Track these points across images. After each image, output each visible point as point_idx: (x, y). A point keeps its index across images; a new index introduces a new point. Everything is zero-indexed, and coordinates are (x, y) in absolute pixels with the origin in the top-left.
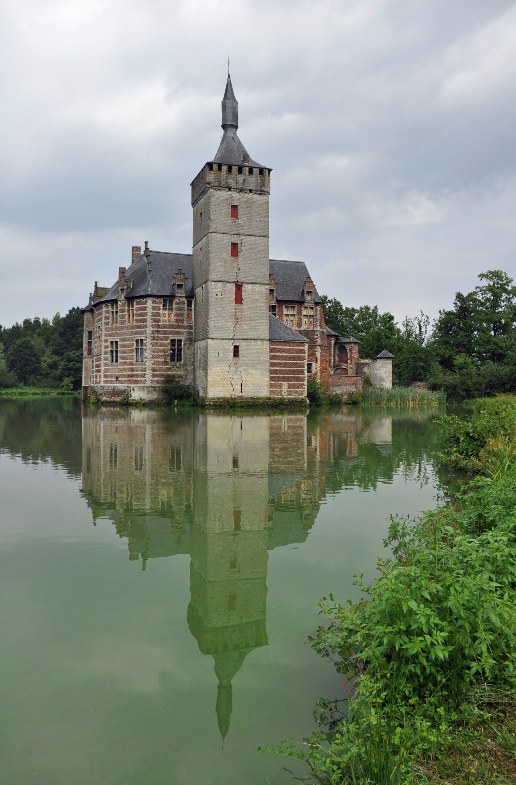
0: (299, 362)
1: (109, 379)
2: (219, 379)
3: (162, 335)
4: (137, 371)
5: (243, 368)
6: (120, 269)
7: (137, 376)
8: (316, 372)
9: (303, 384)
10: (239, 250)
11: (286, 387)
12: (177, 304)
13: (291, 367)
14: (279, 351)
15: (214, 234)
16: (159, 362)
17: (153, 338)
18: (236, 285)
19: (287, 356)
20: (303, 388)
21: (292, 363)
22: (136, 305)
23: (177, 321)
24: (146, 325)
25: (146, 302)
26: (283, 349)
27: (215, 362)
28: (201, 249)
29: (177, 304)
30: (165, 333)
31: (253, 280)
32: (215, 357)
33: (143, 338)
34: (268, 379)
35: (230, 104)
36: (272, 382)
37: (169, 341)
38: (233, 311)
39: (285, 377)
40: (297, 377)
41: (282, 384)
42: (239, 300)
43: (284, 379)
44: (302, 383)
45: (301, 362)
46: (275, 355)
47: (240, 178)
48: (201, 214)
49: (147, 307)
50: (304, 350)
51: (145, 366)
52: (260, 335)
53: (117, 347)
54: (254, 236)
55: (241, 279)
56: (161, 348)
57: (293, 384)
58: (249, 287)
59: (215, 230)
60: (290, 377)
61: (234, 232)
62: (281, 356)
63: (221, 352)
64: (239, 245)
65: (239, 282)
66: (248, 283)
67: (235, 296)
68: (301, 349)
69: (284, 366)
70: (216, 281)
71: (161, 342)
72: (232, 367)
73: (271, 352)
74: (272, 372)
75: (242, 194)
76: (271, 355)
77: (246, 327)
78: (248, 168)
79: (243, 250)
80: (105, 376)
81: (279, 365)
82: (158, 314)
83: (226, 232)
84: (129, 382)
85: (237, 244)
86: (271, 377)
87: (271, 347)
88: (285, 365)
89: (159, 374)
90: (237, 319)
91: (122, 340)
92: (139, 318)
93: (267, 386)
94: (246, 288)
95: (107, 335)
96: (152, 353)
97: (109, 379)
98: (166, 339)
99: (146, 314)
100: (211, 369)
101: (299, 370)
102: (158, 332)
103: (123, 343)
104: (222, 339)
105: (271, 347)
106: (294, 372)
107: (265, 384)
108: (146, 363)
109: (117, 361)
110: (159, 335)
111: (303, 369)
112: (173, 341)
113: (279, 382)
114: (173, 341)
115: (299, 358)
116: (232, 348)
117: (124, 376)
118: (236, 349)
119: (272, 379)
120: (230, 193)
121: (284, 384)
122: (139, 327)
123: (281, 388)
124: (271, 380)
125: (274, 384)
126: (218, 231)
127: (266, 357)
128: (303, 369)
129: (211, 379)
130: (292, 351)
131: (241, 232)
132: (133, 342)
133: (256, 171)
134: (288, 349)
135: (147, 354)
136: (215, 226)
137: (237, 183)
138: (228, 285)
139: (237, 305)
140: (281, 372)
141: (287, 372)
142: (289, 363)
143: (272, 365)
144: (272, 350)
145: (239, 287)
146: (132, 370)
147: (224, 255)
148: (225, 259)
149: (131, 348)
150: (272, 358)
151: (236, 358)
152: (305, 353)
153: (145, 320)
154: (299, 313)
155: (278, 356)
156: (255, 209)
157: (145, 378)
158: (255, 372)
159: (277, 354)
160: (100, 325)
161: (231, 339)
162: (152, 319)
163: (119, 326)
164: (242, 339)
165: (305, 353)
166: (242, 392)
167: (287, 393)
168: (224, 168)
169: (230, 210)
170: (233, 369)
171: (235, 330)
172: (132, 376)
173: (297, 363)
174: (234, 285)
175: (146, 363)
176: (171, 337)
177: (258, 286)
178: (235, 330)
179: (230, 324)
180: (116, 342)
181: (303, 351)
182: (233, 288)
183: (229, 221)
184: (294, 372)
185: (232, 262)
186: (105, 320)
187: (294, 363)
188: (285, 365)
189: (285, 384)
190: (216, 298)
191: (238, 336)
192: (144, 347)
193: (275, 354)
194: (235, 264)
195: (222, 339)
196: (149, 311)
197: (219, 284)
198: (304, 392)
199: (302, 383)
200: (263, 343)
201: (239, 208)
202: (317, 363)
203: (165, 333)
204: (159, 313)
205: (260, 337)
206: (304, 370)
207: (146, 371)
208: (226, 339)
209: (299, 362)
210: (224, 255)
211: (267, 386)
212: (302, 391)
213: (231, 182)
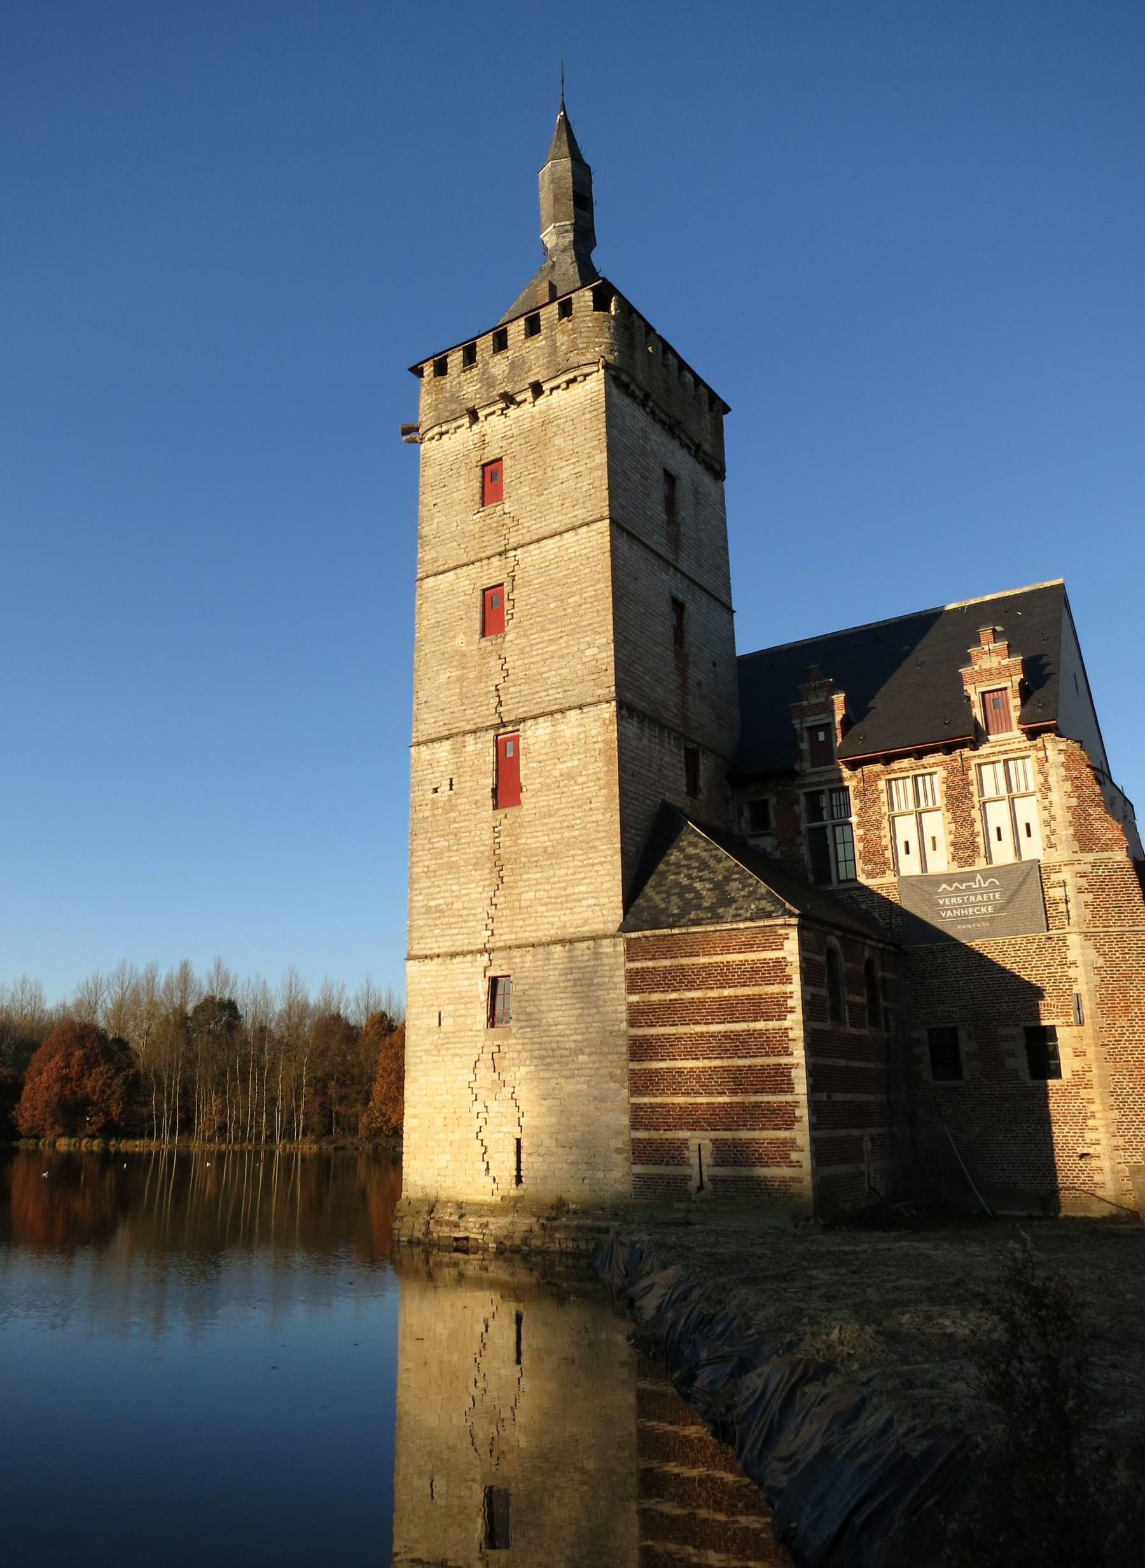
2: (439, 1122)
9: (791, 1144)
10: (507, 605)
15: (431, 580)
19: (702, 1001)
20: (791, 1164)
26: (682, 967)
27: (426, 1051)
31: (552, 697)
32: (429, 1030)
34: (626, 1120)
38: (487, 836)
40: (757, 1105)
41: (685, 1142)
44: (783, 1134)
45: (772, 1024)
46: (650, 1004)
50: (780, 965)
52: (586, 921)
58: (540, 732)
61: (489, 553)
63: (447, 1009)
64: (507, 588)
66: (535, 717)
68: (764, 962)
70: (433, 741)
76: (630, 1005)
77: (531, 895)
86: (636, 1108)
101: (763, 1068)
104: (453, 955)
111: (784, 1060)
115: (757, 1008)
116: (483, 986)
125: (650, 1142)
126: (441, 569)
128: (784, 1060)
137: (488, 381)
142: (713, 1035)
147: (460, 638)
148: (464, 655)
152: (788, 980)
155: (660, 1004)
156: (558, 441)
159: (656, 997)
161: (481, 952)
164: (518, 947)
165: (788, 980)
167: (708, 1185)
170: (486, 1075)
171: (492, 911)
177: (573, 715)
178: (492, 911)
183: (474, 521)
185: (483, 655)
190: (434, 802)
191: (505, 936)
193: (646, 997)
194: (494, 663)
195: (453, 955)
201: (507, 462)
205: (586, 930)
210: (460, 641)
211: (618, 1151)
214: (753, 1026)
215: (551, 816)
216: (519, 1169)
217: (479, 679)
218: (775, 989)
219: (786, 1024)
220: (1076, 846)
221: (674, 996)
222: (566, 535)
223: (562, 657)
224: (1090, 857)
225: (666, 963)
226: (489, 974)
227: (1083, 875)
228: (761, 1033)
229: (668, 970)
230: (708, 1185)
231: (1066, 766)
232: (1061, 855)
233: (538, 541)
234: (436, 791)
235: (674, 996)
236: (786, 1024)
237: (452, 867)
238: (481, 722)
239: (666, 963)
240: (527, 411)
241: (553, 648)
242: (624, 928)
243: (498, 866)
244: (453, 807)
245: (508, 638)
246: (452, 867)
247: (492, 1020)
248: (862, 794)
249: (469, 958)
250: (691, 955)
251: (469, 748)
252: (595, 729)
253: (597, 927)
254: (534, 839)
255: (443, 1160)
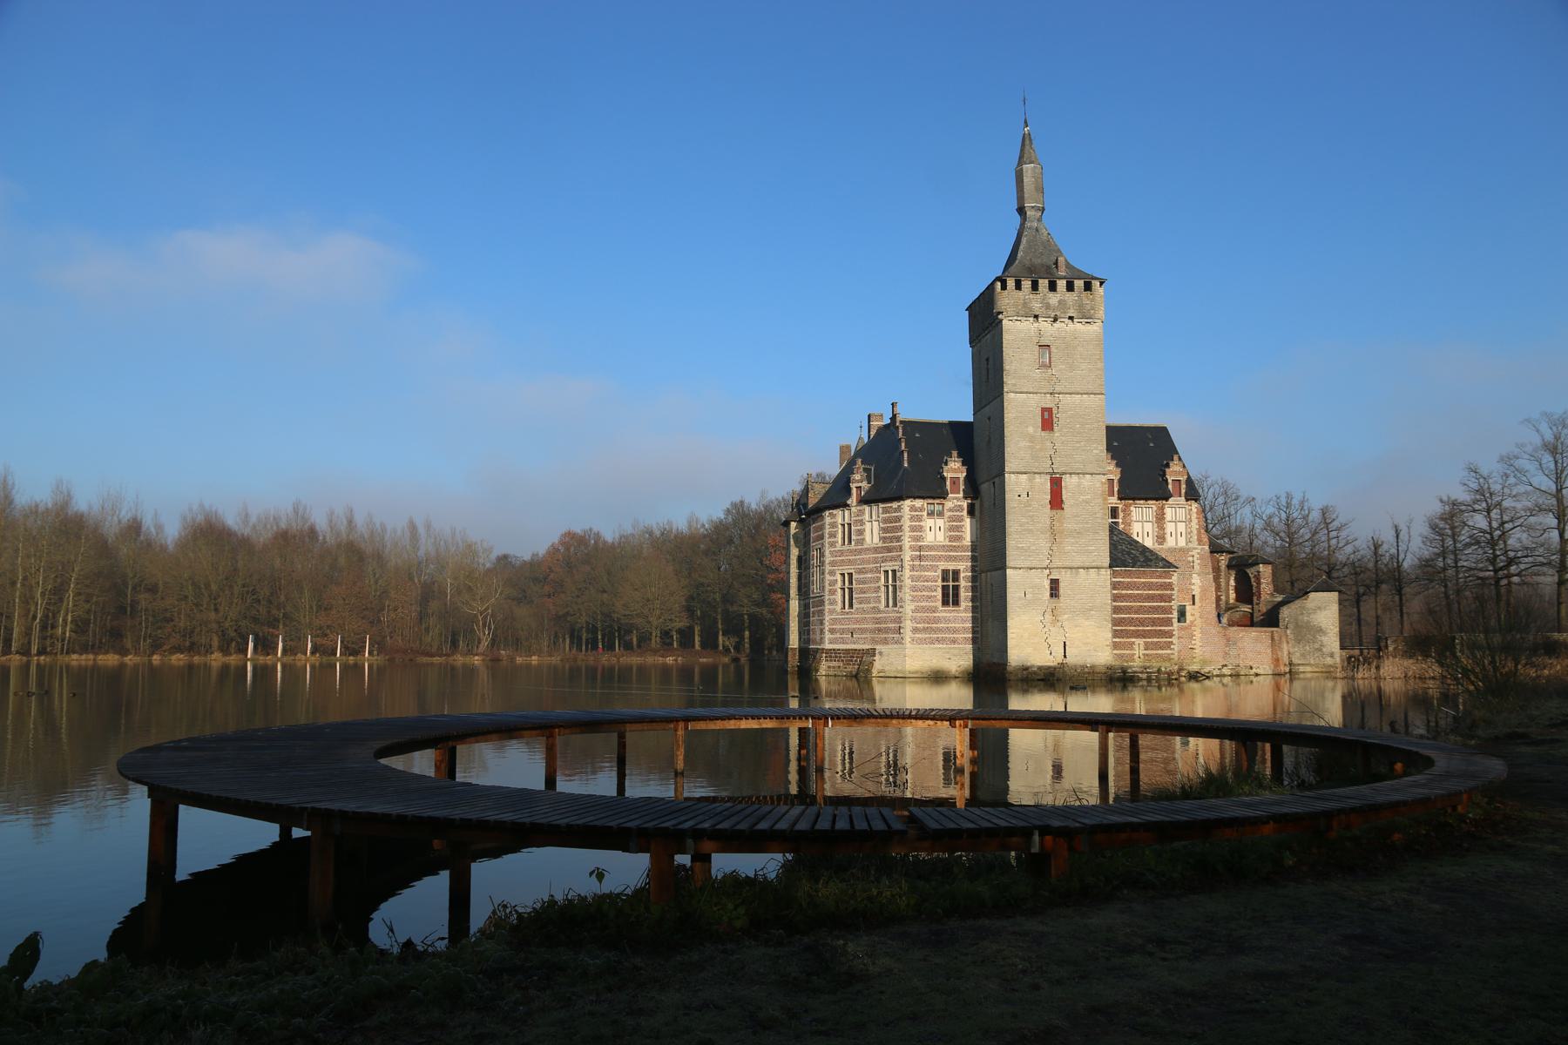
0: (1163, 604)
1: (838, 635)
3: (927, 563)
4: (885, 622)
5: (1066, 616)
6: (842, 448)
7: (887, 630)
8: (1192, 622)
10: (1055, 420)
11: (1142, 647)
12: (950, 510)
13: (1149, 613)
14: (1128, 586)
16: (923, 607)
17: (913, 568)
18: (1052, 479)
21: (1150, 607)
22: (883, 513)
23: (952, 539)
24: (901, 547)
25: (899, 509)
28: (989, 419)
29: (950, 510)
30: (935, 558)
31: (1078, 467)
32: (1020, 599)
33: (897, 568)
34: (1110, 635)
35: (1029, 172)
36: (1117, 640)
37: (939, 573)
39: (1138, 630)
40: (1160, 630)
41: (1134, 643)
42: (1056, 501)
43: (1138, 635)
44: (1170, 640)
45: (1167, 604)
47: (1054, 299)
48: (987, 360)
49: (902, 517)
51: (898, 615)
52: (1094, 561)
53: (851, 582)
54: (1078, 394)
55: (1059, 468)
56: (926, 584)
57: (1152, 643)
59: (1012, 390)
60: (1148, 630)
62: (1130, 596)
64: (1055, 411)
65: (1056, 473)
66: (1071, 474)
67: (1049, 497)
69: (1136, 613)
71: (926, 573)
72: (1047, 616)
73: (1114, 588)
74: (1116, 622)
75: (1057, 325)
78: (1064, 282)
79: (1061, 419)
80: (832, 631)
81: (1129, 610)
82: (920, 529)
83: (1032, 390)
84: (874, 641)
85: (1050, 410)
86: (1116, 631)
87: (1114, 580)
88: (1139, 610)
89: (924, 628)
90: (1054, 534)
91: (860, 572)
92: (888, 535)
93: (1107, 646)
94: (1069, 483)
95: (833, 564)
96: (912, 593)
97: (838, 635)
98: (934, 568)
99: (900, 529)
100: (1013, 619)
102: (920, 558)
103: (862, 576)
104: (1031, 569)
105: (1114, 580)
106: (1154, 622)
107: (1105, 644)
108: (901, 610)
109: (851, 606)
110: (922, 563)
112: (945, 573)
113: (1128, 640)
114: (945, 573)
116: (1047, 584)
117: (863, 631)
118: (1055, 586)
119: (1116, 634)
120: (1036, 325)
121: (1137, 643)
122: (889, 550)
123: (1132, 649)
124: (1115, 636)
125: (1120, 642)
127: (1105, 597)
129: (1014, 636)
130: (1150, 586)
131: (1058, 389)
132: (878, 575)
133: (1079, 284)
134: (1143, 583)
135: (906, 594)
136: (1013, 382)
137: (1048, 306)
138: (1038, 479)
139: (1054, 512)
140: (1131, 622)
141: (1142, 622)
143: (1116, 610)
144: (1115, 586)
145: (1056, 484)
146: (878, 621)
149: (877, 585)
150: (1115, 598)
151: (1055, 600)
153: (898, 539)
154: (1160, 518)
156: (1079, 349)
157: (900, 633)
158: (1087, 623)
159: (1124, 592)
160: (819, 546)
162: (910, 537)
163: (855, 548)
166: (1065, 656)
167: (1142, 657)
168: (1027, 284)
169: (1036, 353)
170: (1048, 616)
171: (1051, 552)
172: (879, 630)
173: (1159, 606)
174: (1048, 477)
175: (901, 610)
176: (943, 565)
178: (1051, 552)
179: (1043, 543)
180: (850, 575)
181: (1169, 586)
182: (1044, 483)
184: (1154, 622)
186: (830, 537)
187: (1154, 607)
188: (1139, 610)
189: (1140, 642)
191: (1056, 563)
192: (898, 583)
194: (1049, 444)
196: (906, 523)
197: (1025, 476)
198: (1172, 657)
199: (1170, 640)
200: (1099, 575)
201: (1053, 349)
202: (1194, 604)
203: (935, 558)
204: (921, 527)
205: (1094, 564)
206: (1172, 618)
207: (901, 622)
208: (1037, 568)
209: (1163, 604)
210: (1031, 430)
211: (1107, 646)
212: (1169, 654)
213: (1036, 306)
214: (1159, 604)
215: (1078, 517)
216: (1065, 653)
217: (1041, 450)
218: (1169, 592)
219: (1171, 604)
220: (1197, 543)
221: (1132, 592)
222: (1084, 396)
223: (1084, 450)
224: (1200, 547)
225: (1129, 580)
226: (1050, 577)
227: (1198, 553)
228: (1163, 607)
229: (1129, 583)
230: (1142, 657)
231: (1197, 513)
232: (1195, 544)
233: (1070, 394)
234: (1019, 496)
235: (1132, 592)
236: (1171, 604)
237: (1030, 531)
238: (1042, 470)
239: (1129, 580)
240: (1063, 326)
241: (1078, 445)
242: (1110, 567)
243: (1053, 534)
244: (1030, 505)
245: (1056, 435)
246: (1030, 531)
247: (1052, 595)
248: (1124, 511)
249: (1039, 570)
250: (1138, 578)
251: (1038, 480)
252: (1098, 485)
253: (1099, 564)
254: (1069, 525)
255: (1029, 650)
